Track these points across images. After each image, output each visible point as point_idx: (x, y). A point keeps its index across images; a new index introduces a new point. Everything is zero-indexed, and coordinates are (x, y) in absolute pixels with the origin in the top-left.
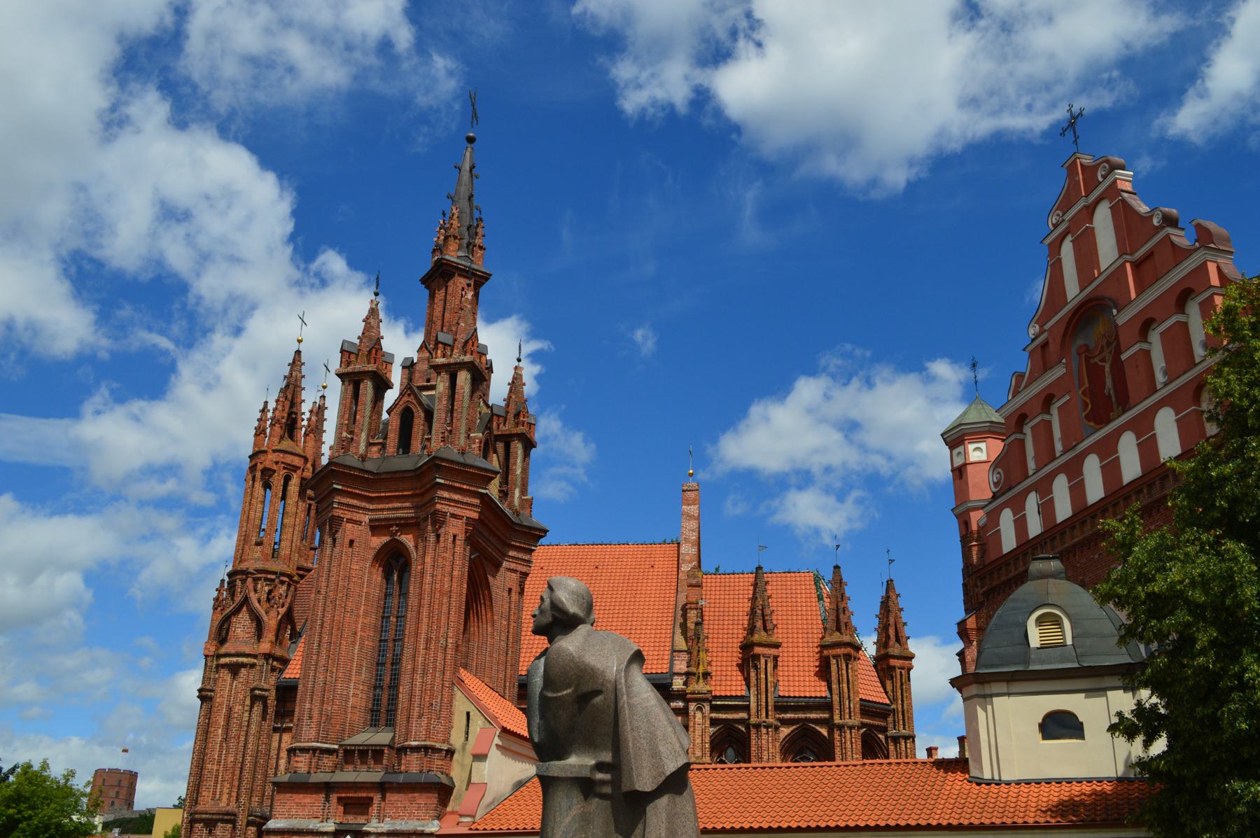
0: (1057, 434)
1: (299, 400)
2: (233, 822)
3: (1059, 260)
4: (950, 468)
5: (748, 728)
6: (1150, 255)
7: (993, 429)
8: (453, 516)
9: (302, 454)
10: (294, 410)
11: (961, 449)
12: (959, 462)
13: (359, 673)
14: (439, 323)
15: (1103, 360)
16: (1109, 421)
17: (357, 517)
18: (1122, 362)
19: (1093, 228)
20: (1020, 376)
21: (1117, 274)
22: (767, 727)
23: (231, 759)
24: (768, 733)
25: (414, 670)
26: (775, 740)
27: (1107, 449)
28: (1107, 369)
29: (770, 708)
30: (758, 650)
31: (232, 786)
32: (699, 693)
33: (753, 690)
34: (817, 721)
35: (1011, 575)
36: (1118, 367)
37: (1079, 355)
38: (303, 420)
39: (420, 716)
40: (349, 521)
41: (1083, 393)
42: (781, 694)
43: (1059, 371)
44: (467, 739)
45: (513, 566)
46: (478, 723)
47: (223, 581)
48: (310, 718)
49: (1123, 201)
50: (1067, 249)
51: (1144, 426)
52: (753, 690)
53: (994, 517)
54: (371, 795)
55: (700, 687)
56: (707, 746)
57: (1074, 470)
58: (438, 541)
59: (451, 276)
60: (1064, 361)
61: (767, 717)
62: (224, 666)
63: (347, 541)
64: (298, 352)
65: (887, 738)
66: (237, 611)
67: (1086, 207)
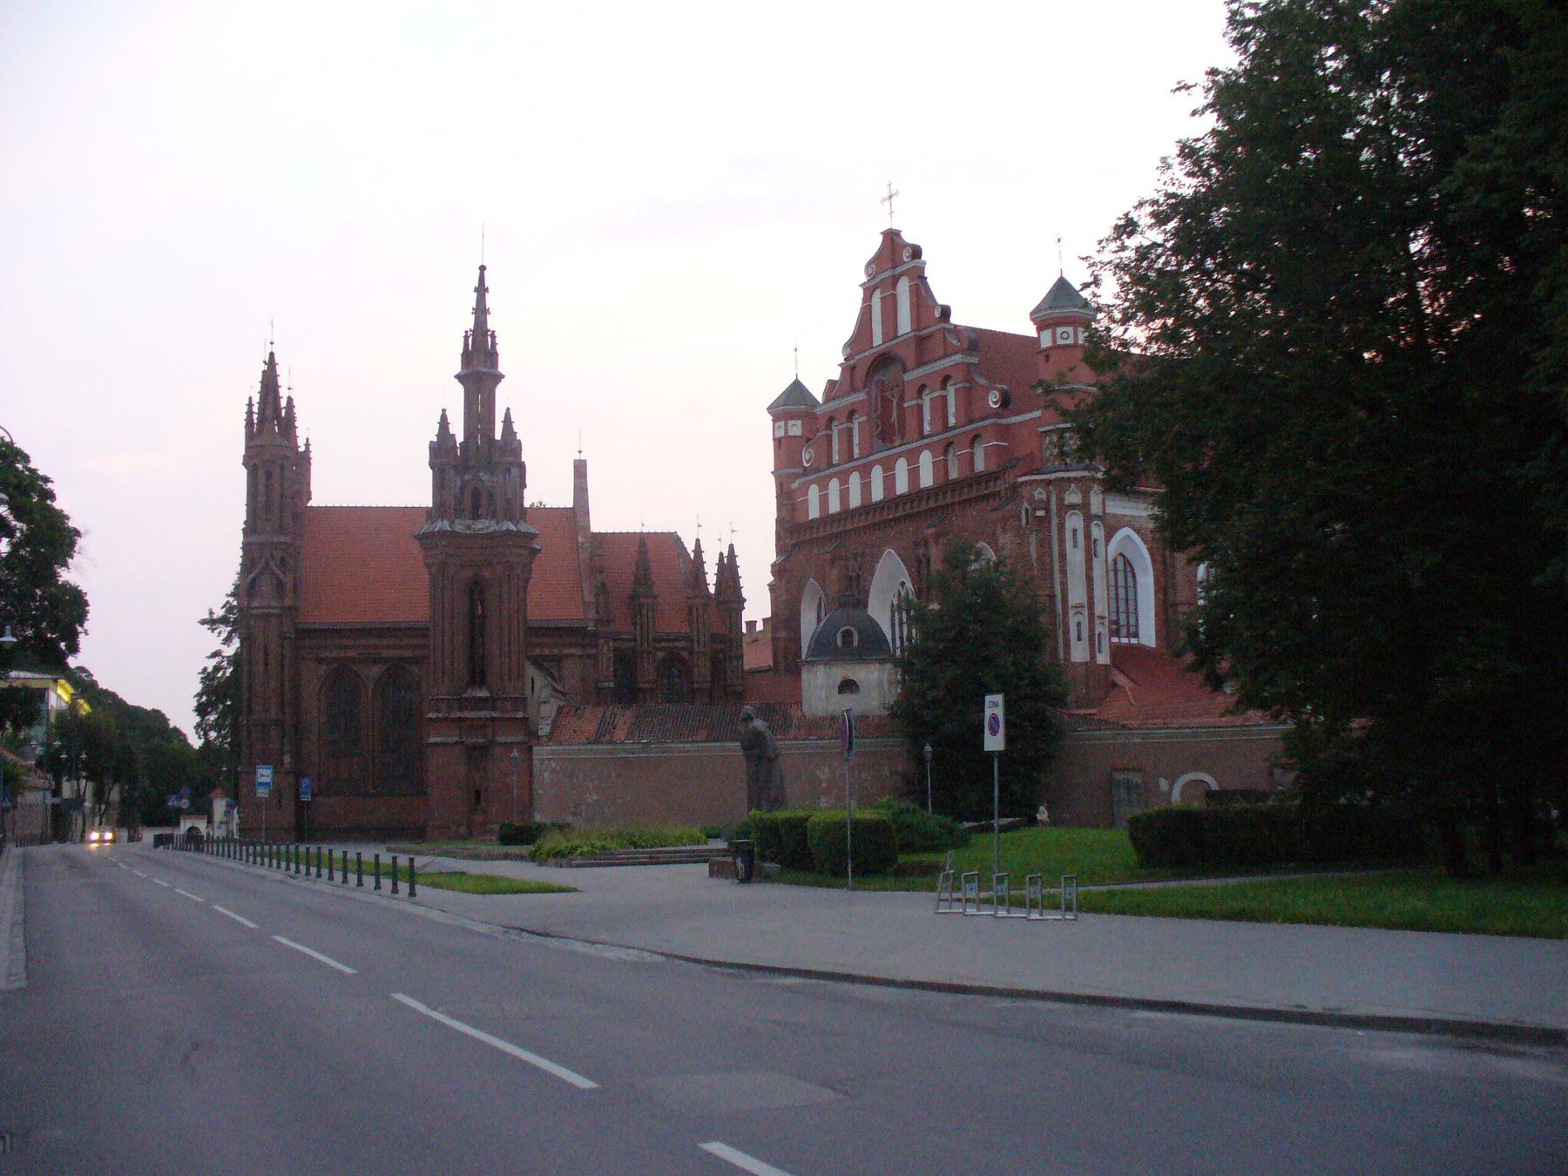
4: (772, 437)
6: (929, 337)
11: (782, 423)
12: (781, 433)
23: (273, 683)
27: (888, 466)
28: (895, 404)
34: (683, 649)
37: (877, 386)
43: (862, 396)
44: (533, 691)
46: (539, 682)
50: (877, 297)
51: (912, 458)
52: (638, 628)
55: (602, 629)
64: (272, 355)
65: (725, 656)
67: (893, 276)
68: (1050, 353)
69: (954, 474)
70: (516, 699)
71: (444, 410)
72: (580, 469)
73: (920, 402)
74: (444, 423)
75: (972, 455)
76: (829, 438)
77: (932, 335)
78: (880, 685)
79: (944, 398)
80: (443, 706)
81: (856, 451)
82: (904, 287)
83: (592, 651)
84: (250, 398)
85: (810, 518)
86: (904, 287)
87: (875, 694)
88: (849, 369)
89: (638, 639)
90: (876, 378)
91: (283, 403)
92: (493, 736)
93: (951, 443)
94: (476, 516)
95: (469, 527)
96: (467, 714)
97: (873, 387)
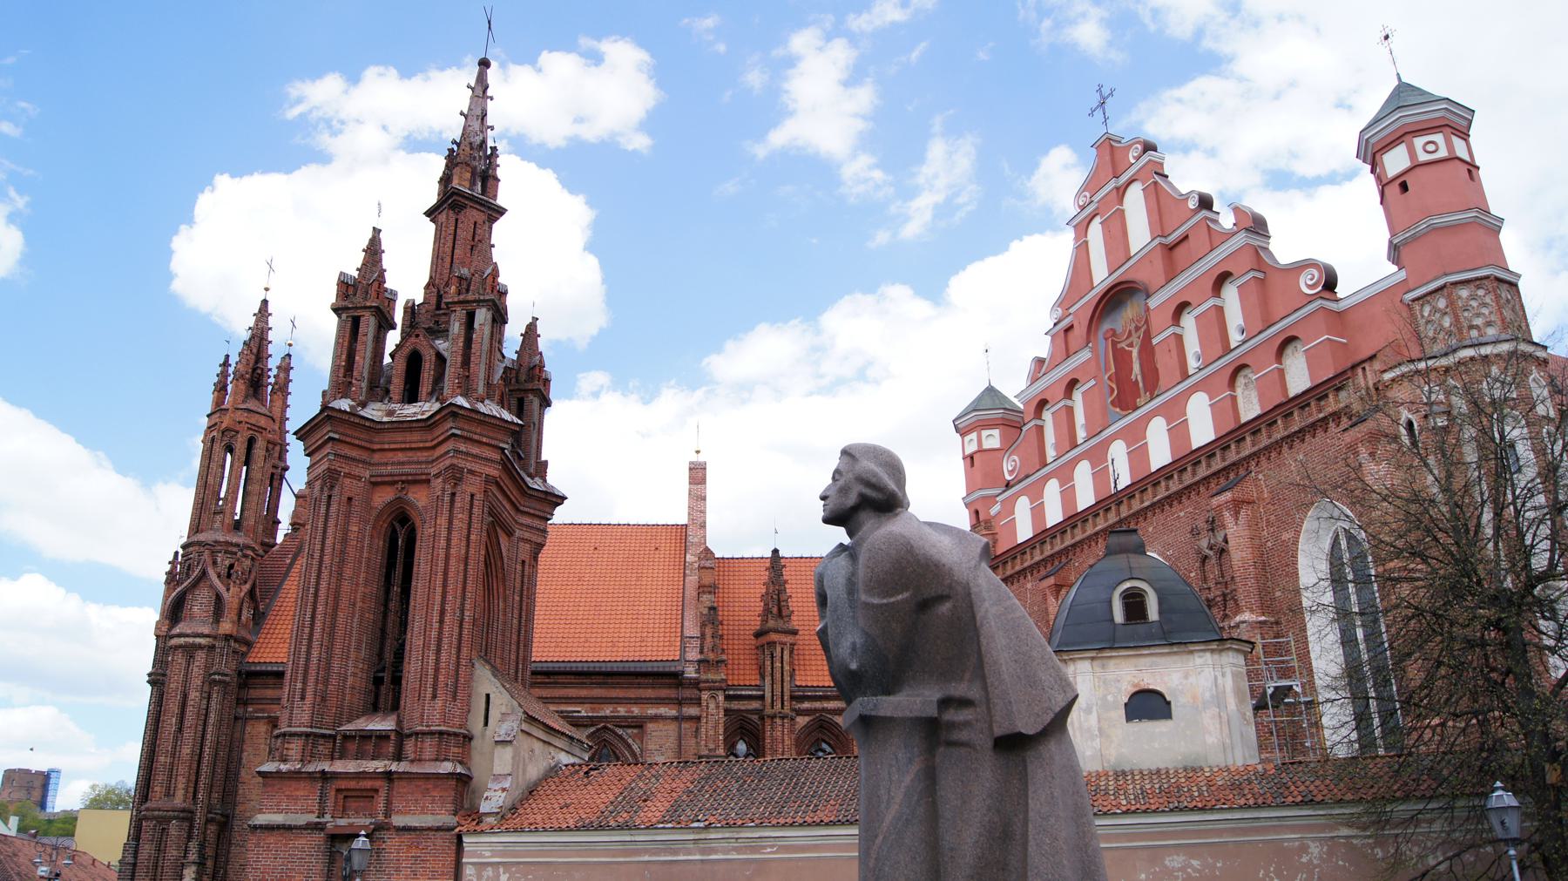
0: (1080, 418)
1: (265, 355)
2: (191, 820)
3: (1086, 243)
4: (961, 456)
5: (762, 718)
7: (1006, 416)
8: (471, 472)
9: (268, 414)
10: (260, 365)
11: (974, 435)
12: (971, 448)
13: (358, 649)
14: (448, 260)
15: (1131, 345)
16: (1136, 408)
17: (357, 471)
18: (1153, 348)
19: (1123, 211)
20: (1040, 362)
21: (1147, 257)
22: (783, 718)
23: (186, 750)
24: (783, 726)
25: (426, 646)
26: (791, 731)
27: (1135, 438)
29: (786, 698)
30: (774, 637)
31: (189, 781)
32: (713, 682)
33: (768, 680)
35: (1026, 565)
36: (1147, 350)
37: (1106, 339)
38: (269, 377)
39: (434, 697)
40: (348, 475)
41: (1110, 378)
42: (798, 683)
43: (1085, 355)
44: (486, 724)
45: (527, 535)
47: (177, 553)
48: (303, 698)
49: (1156, 183)
50: (1096, 231)
52: (768, 680)
53: (1009, 507)
54: (377, 784)
56: (721, 738)
57: (1098, 456)
58: (452, 502)
59: (465, 207)
60: (1090, 345)
61: (782, 708)
62: (177, 647)
63: (344, 499)
64: (265, 302)
66: (195, 585)
67: (1117, 189)
68: (1409, 179)
69: (1250, 408)
70: (441, 733)
71: (376, 231)
72: (698, 474)
73: (1178, 330)
74: (374, 251)
75: (1281, 372)
76: (1040, 429)
77: (1187, 237)
78: (1219, 700)
79: (1220, 310)
80: (295, 747)
81: (1081, 434)
82: (1135, 198)
83: (692, 711)
84: (227, 356)
85: (1020, 541)
86: (1135, 203)
87: (1208, 719)
88: (1064, 335)
89: (768, 695)
90: (1106, 326)
91: (273, 363)
92: (387, 814)
93: (1243, 367)
94: (411, 396)
95: (391, 413)
96: (339, 766)
97: (1101, 343)
